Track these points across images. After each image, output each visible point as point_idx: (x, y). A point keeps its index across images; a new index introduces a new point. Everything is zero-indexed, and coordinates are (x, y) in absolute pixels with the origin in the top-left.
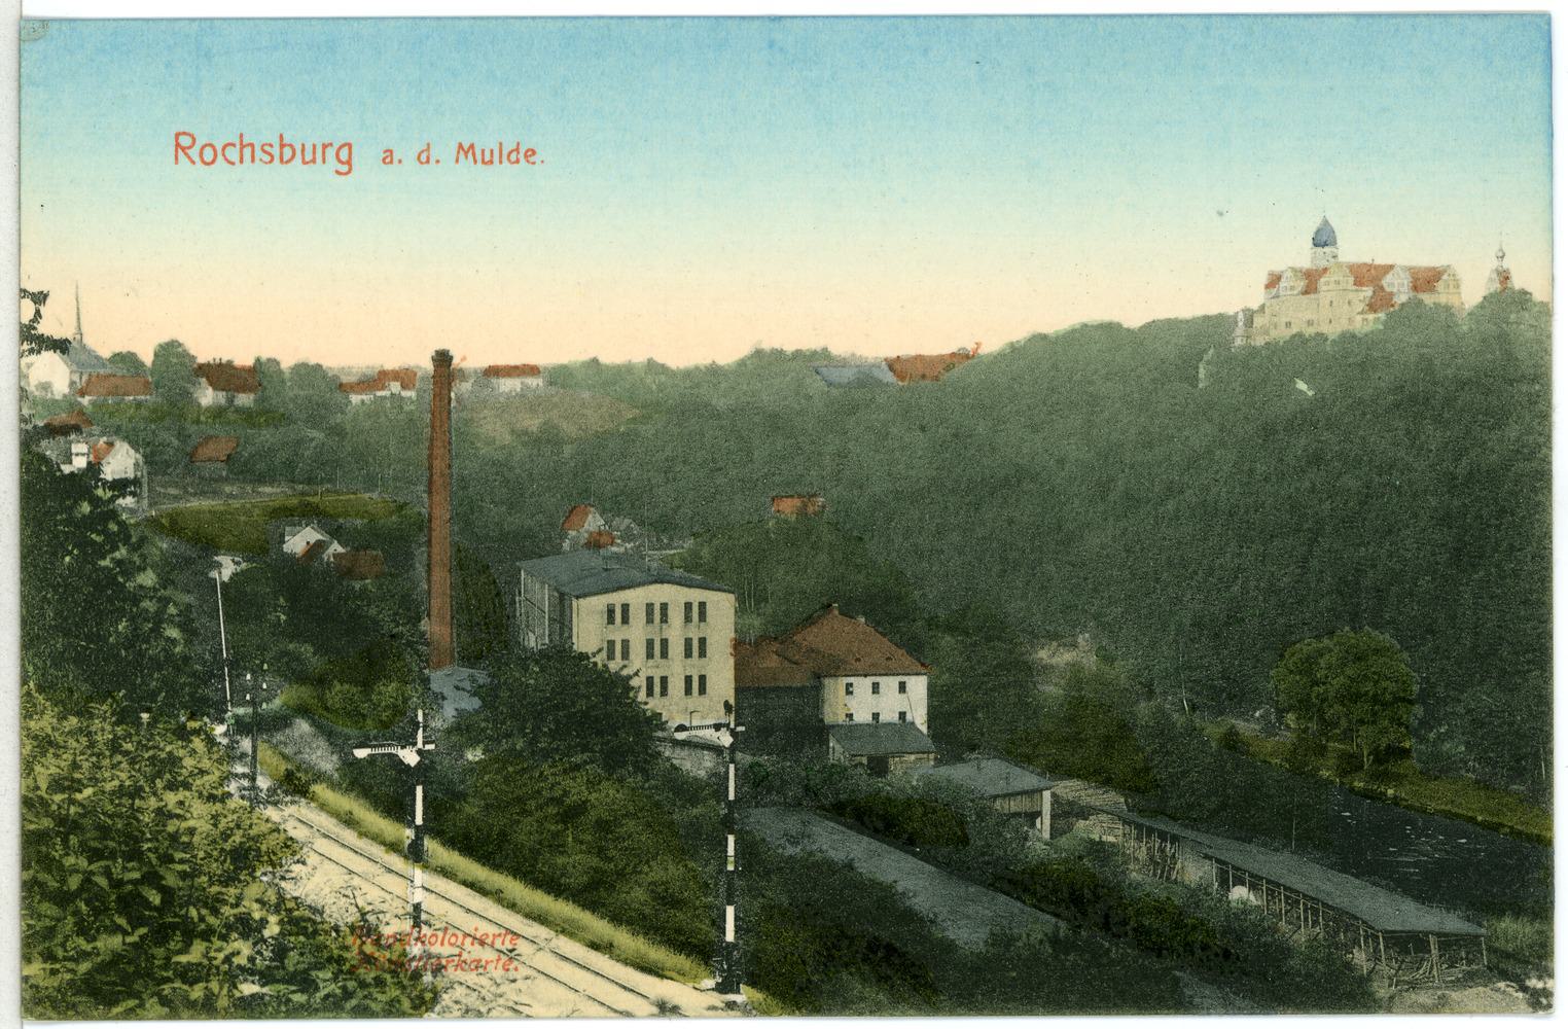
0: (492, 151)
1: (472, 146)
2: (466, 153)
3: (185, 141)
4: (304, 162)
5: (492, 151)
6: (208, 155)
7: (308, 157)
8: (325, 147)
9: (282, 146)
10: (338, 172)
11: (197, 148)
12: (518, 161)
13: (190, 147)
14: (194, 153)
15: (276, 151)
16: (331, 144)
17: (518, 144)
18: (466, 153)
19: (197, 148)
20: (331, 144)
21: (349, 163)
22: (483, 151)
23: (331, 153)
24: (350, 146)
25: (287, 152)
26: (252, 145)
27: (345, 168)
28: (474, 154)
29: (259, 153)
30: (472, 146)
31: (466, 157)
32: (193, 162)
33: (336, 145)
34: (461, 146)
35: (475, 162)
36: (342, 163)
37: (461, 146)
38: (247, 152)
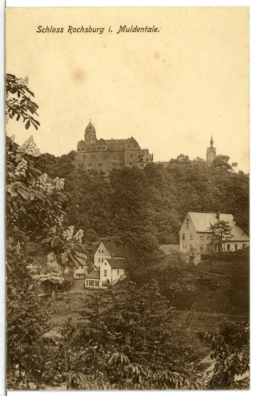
0: (129, 29)
4: (93, 32)
5: (129, 29)
8: (98, 29)
12: (135, 31)
14: (72, 30)
17: (137, 26)
21: (102, 32)
22: (127, 29)
23: (99, 30)
24: (103, 29)
25: (90, 30)
26: (83, 29)
29: (85, 30)
36: (101, 31)
38: (82, 30)
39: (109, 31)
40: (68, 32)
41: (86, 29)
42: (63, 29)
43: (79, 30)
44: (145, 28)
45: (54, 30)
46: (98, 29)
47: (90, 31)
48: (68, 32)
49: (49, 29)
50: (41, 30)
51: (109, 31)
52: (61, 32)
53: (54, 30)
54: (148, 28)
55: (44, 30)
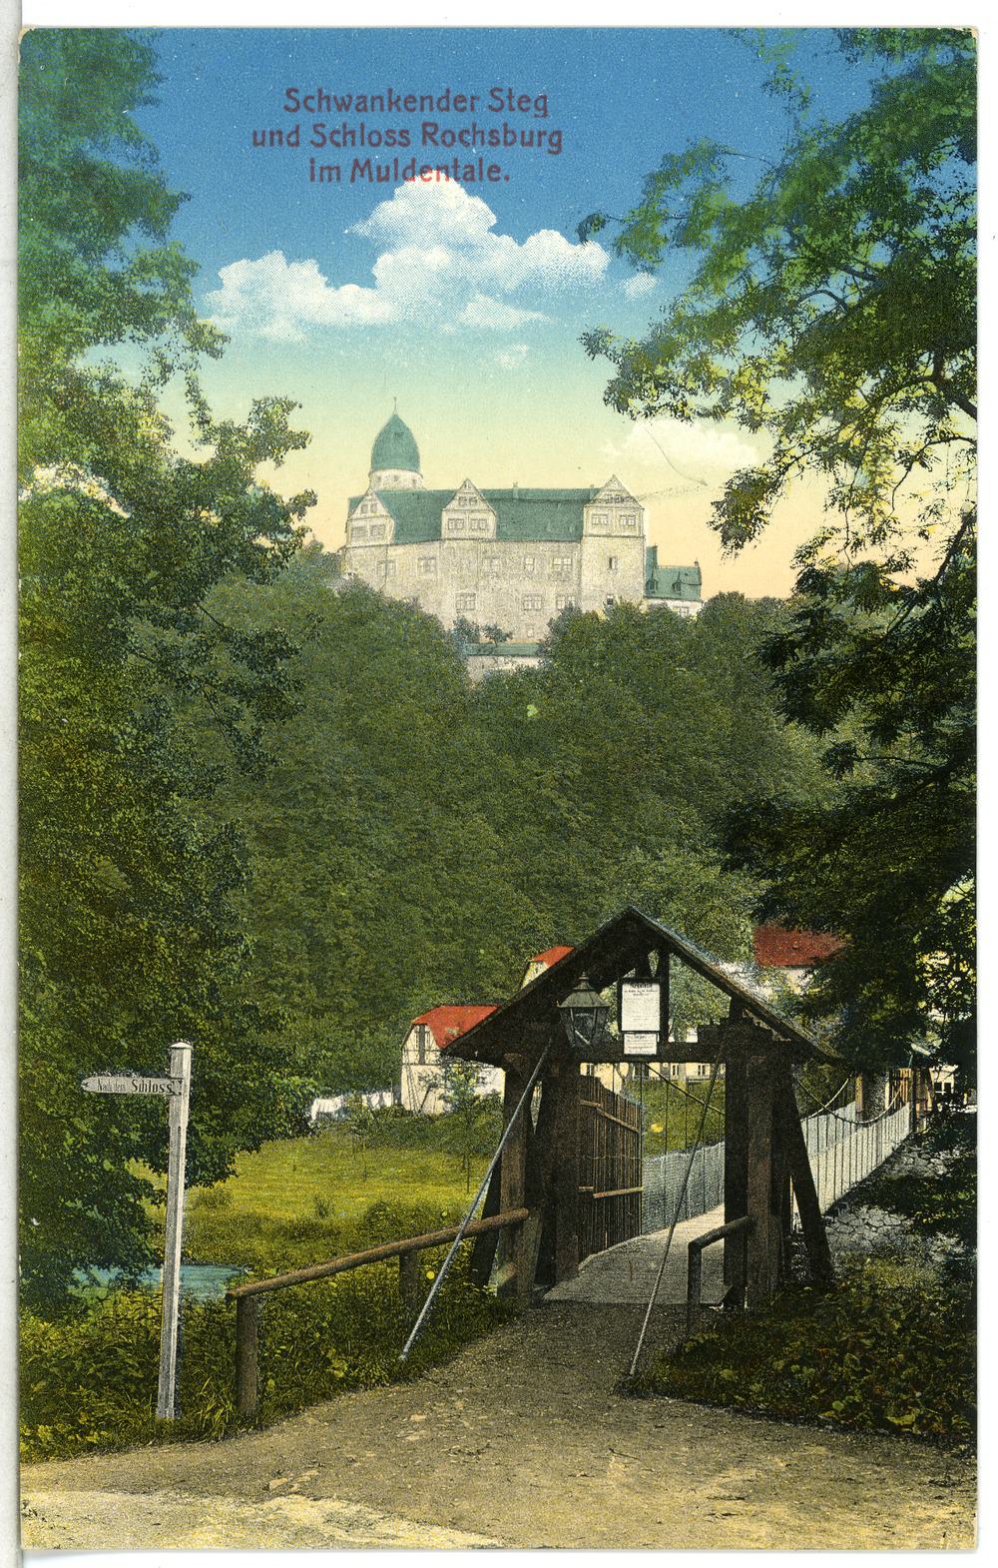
0: (388, 168)
1: (368, 162)
2: (362, 171)
3: (430, 129)
5: (388, 168)
6: (448, 139)
7: (527, 139)
9: (506, 132)
10: (550, 152)
11: (439, 133)
13: (434, 133)
15: (502, 138)
16: (545, 133)
18: (362, 171)
19: (439, 133)
20: (545, 133)
22: (379, 169)
23: (545, 139)
24: (558, 133)
25: (510, 138)
27: (555, 149)
28: (370, 173)
29: (487, 138)
30: (368, 162)
31: (362, 175)
32: (436, 143)
33: (549, 133)
34: (356, 163)
35: (371, 180)
37: (356, 163)
39: (313, 179)
40: (424, 142)
41: (492, 132)
42: (407, 132)
43: (468, 138)
44: (451, 163)
45: (375, 139)
46: (540, 134)
47: (509, 141)
48: (424, 142)
49: (352, 133)
50: (324, 137)
51: (313, 179)
52: (400, 144)
53: (375, 139)
54: (462, 164)
55: (339, 138)
